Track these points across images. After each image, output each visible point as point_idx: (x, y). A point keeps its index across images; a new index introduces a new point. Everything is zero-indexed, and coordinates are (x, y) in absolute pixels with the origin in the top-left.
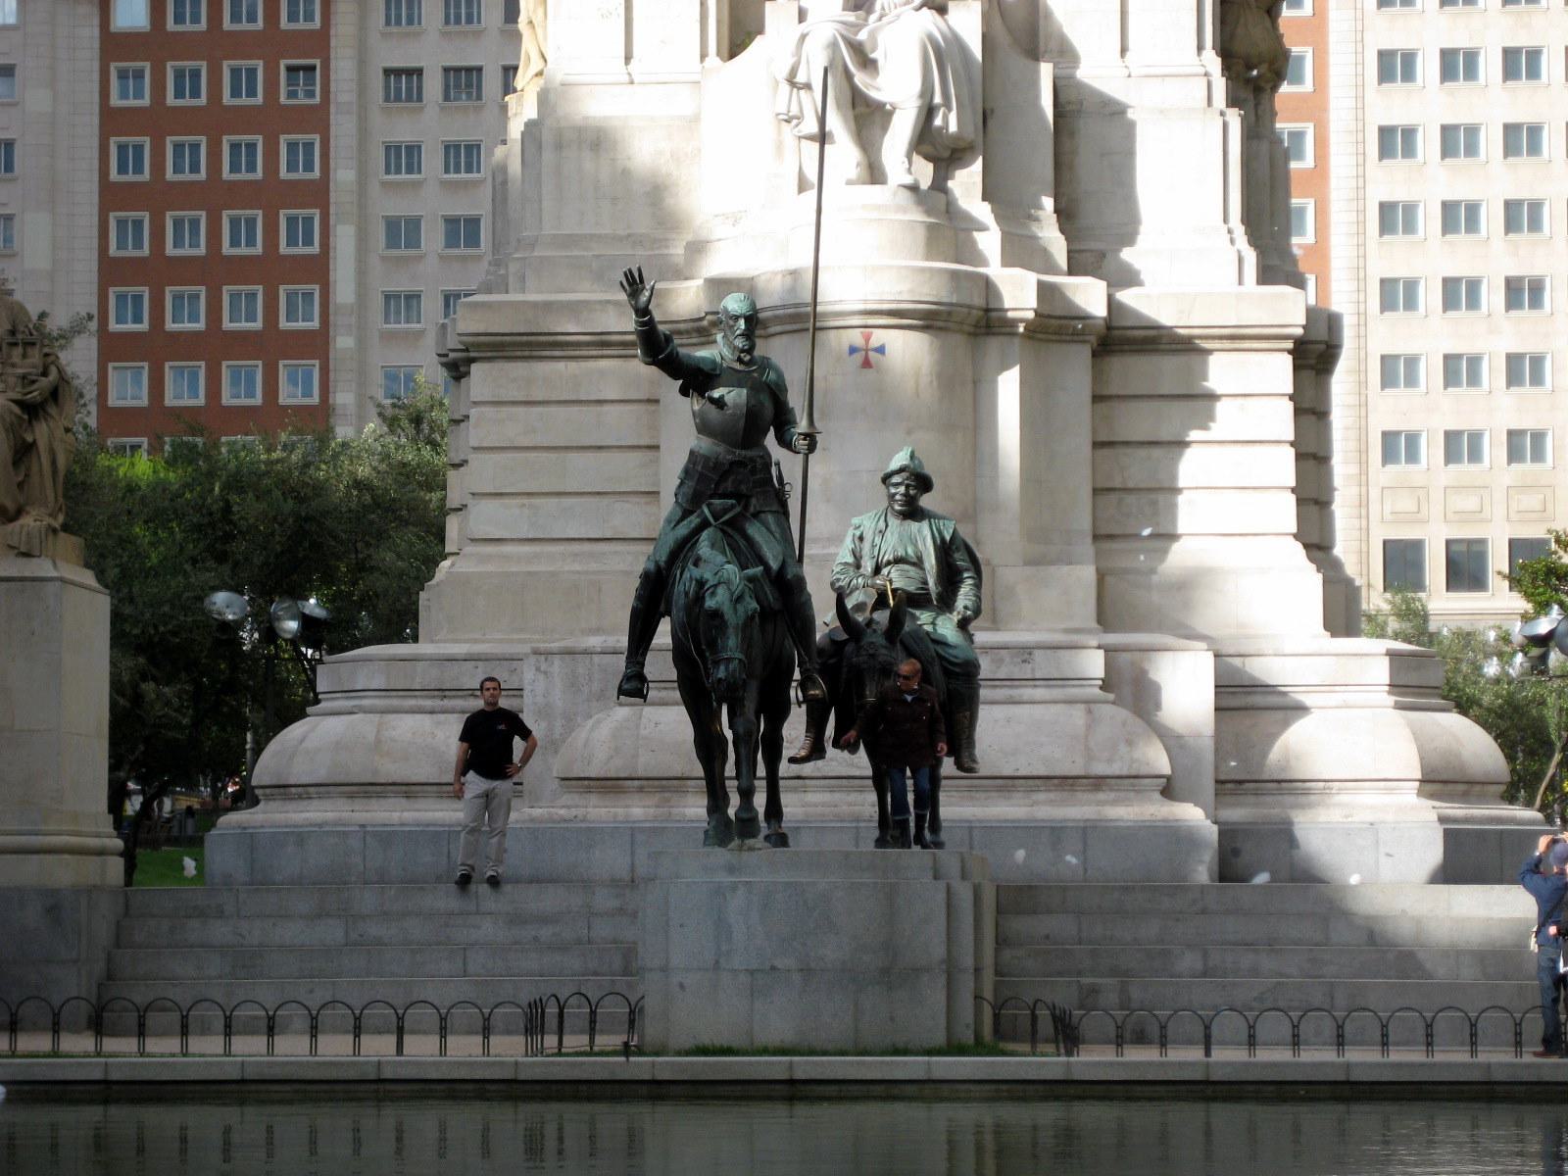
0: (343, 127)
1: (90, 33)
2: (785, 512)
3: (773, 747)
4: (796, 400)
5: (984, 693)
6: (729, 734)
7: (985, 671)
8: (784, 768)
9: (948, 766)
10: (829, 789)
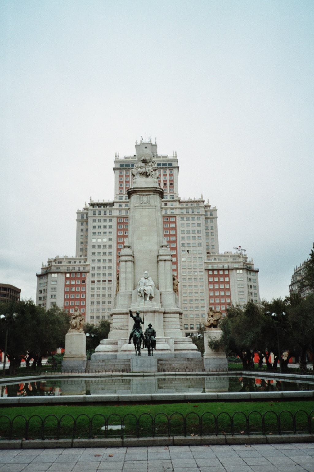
0: (87, 286)
1: (64, 278)
2: (141, 329)
3: (140, 347)
4: (142, 320)
5: (157, 342)
6: (137, 347)
7: (157, 341)
8: (141, 349)
9: (154, 349)
10: (144, 351)
